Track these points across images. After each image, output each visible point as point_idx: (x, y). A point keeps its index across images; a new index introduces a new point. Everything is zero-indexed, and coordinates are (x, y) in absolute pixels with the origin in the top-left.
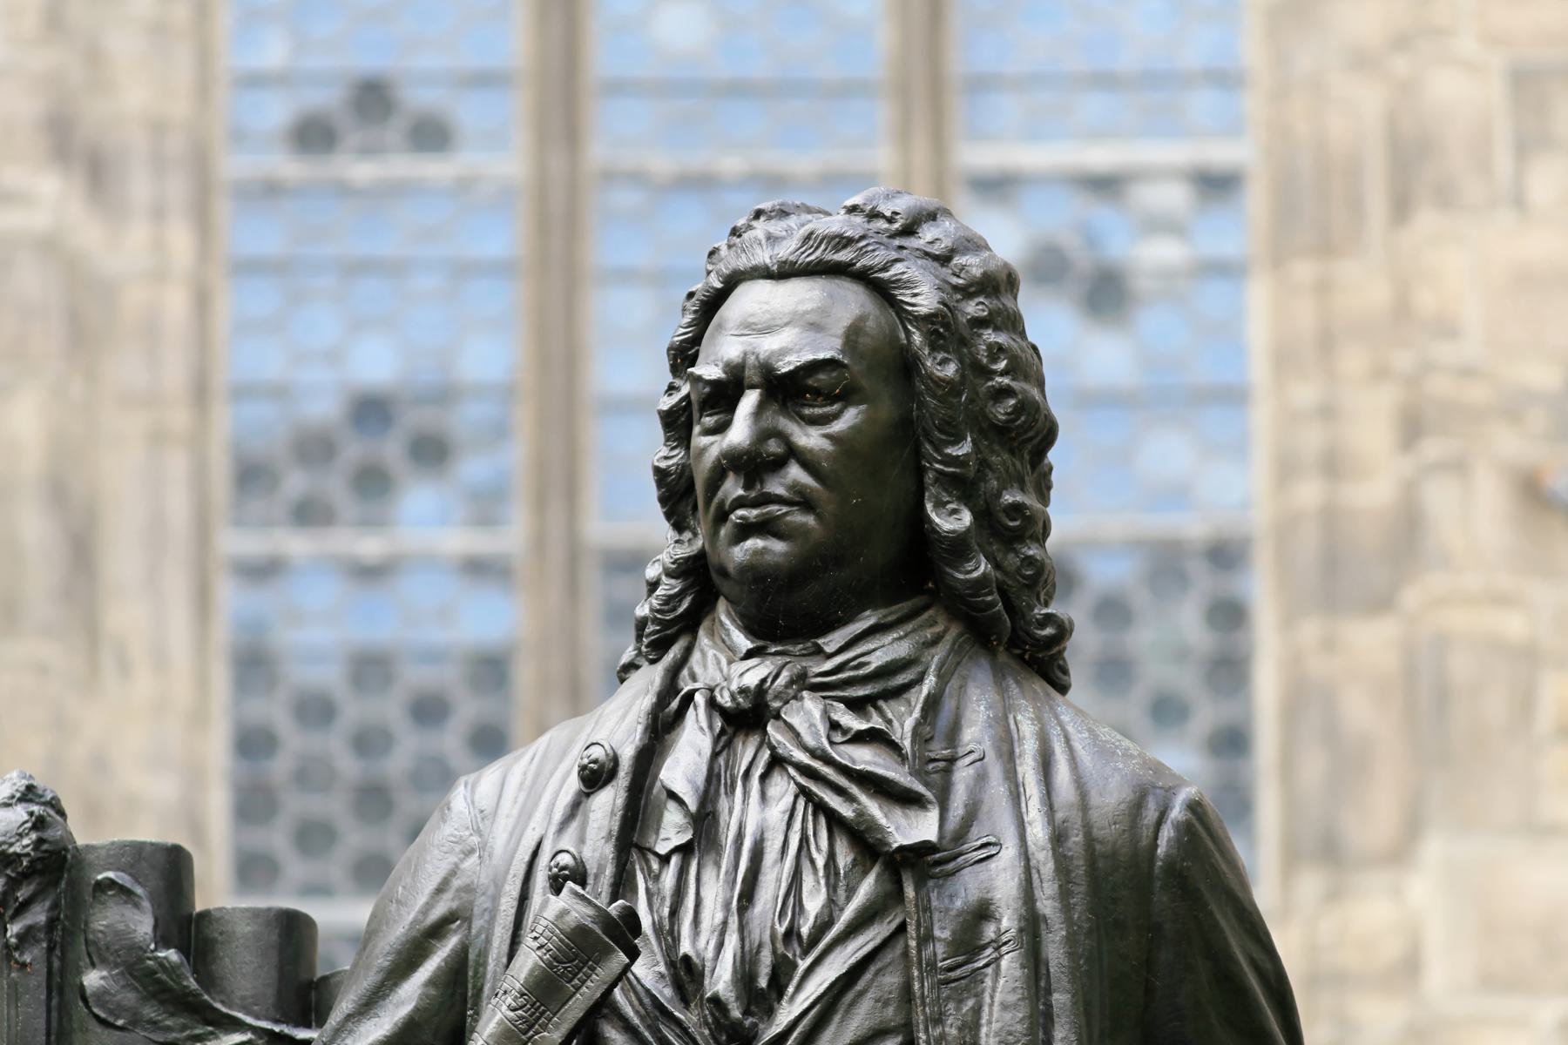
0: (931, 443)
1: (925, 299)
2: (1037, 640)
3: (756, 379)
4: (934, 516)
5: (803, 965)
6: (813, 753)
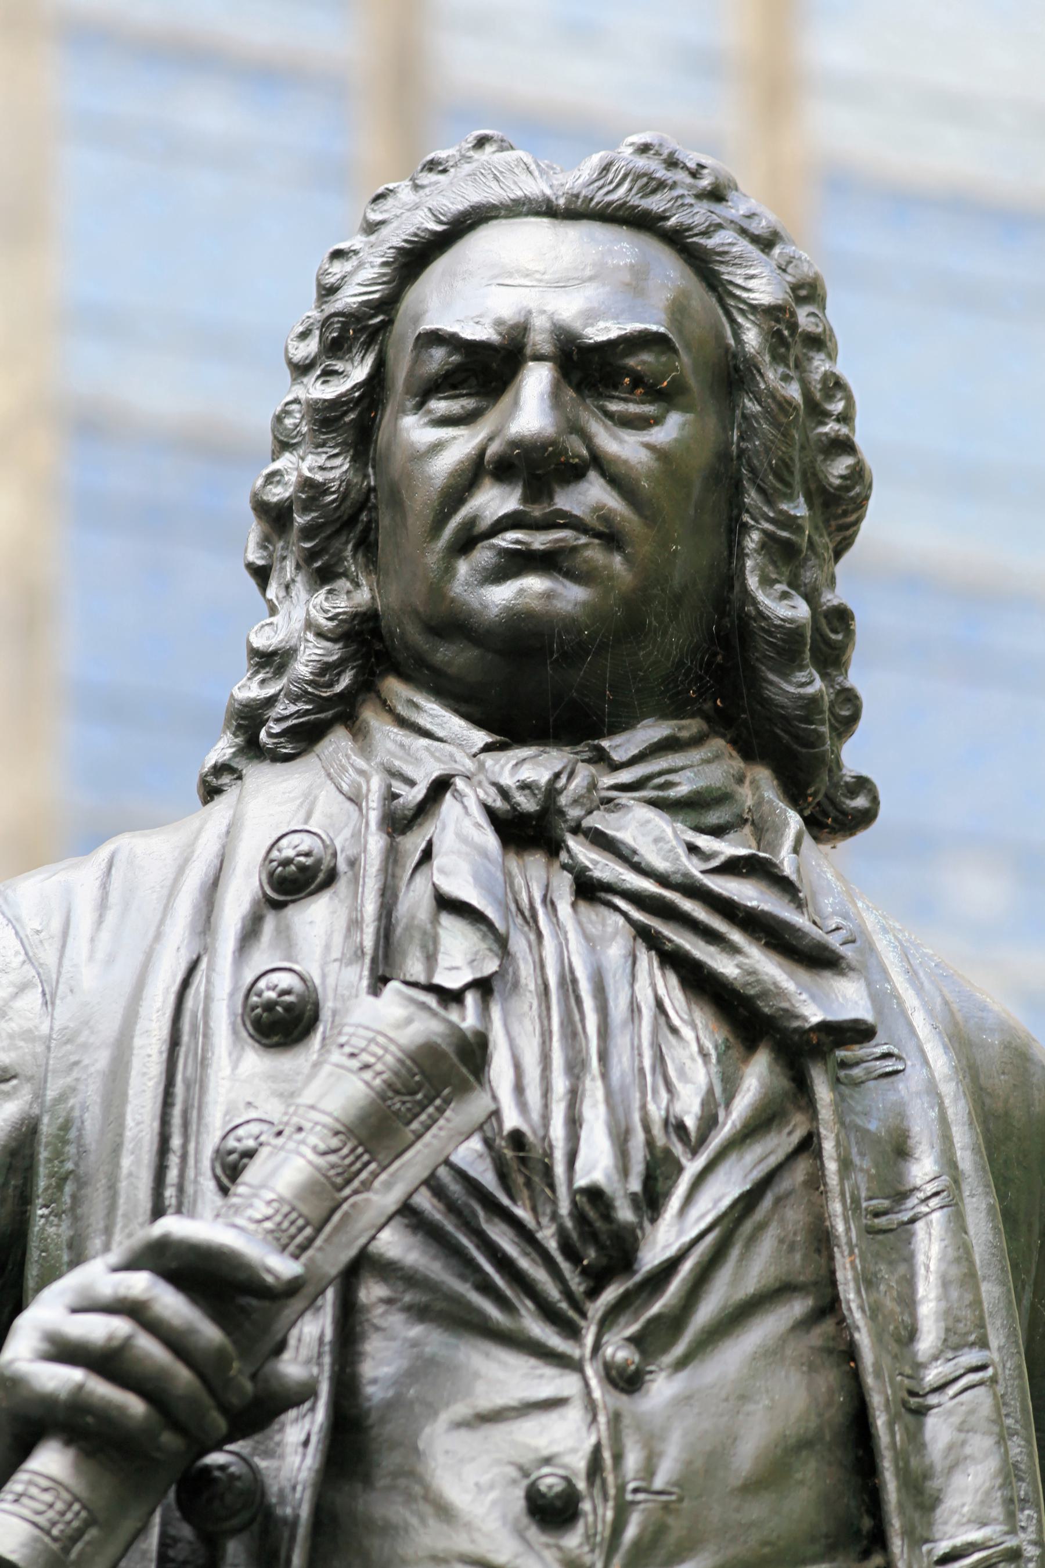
0: (761, 490)
1: (762, 286)
2: (844, 813)
3: (547, 348)
4: (761, 596)
5: (692, 1167)
6: (662, 880)
